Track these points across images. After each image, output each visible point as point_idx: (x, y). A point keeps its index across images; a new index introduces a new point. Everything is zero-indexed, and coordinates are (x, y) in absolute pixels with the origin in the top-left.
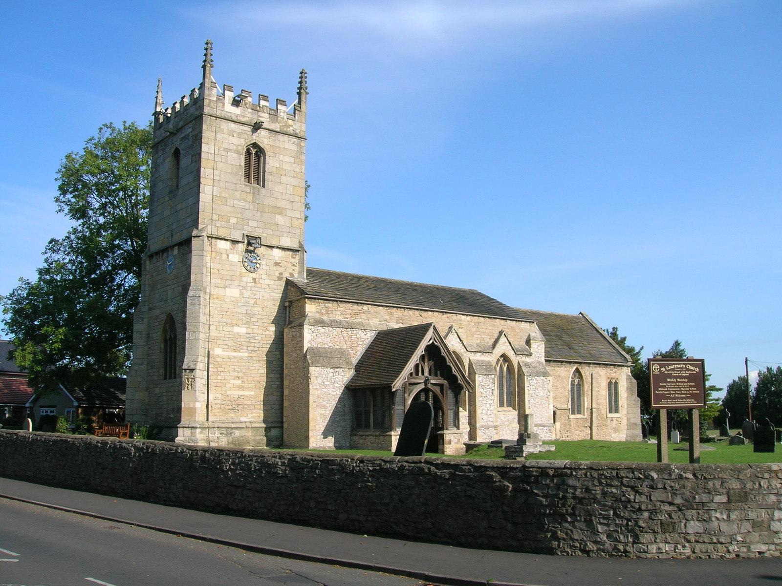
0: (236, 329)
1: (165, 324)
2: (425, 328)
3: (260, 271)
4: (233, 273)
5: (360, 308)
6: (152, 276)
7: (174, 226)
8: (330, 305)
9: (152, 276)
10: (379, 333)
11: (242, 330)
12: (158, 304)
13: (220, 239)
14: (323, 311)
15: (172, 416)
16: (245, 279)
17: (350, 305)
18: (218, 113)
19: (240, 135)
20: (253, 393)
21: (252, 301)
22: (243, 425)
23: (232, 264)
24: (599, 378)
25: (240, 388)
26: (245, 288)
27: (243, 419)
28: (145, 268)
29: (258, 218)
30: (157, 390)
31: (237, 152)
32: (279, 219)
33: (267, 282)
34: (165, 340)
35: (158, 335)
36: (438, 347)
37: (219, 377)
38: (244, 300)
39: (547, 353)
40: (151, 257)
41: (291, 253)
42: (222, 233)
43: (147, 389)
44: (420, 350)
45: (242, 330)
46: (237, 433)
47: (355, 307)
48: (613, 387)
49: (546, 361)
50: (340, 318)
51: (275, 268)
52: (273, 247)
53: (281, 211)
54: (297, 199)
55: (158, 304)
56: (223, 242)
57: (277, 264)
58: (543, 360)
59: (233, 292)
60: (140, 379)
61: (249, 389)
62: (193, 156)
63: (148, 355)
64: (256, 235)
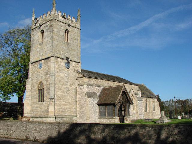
0: (63, 86)
1: (38, 85)
2: (121, 87)
3: (70, 69)
4: (62, 69)
5: (98, 80)
6: (32, 70)
7: (42, 54)
8: (91, 79)
9: (32, 70)
10: (103, 89)
11: (65, 86)
12: (35, 78)
13: (59, 58)
14: (89, 81)
15: (42, 114)
16: (66, 71)
17: (96, 79)
18: (57, 19)
19: (64, 26)
20: (68, 106)
21: (67, 78)
22: (66, 116)
23: (62, 66)
24: (151, 100)
25: (65, 105)
26: (65, 73)
27: (65, 114)
28: (30, 67)
29: (69, 52)
30: (35, 106)
31: (63, 31)
32: (74, 53)
33: (71, 72)
34: (39, 90)
35: (36, 89)
36: (125, 92)
37: (59, 101)
38: (65, 77)
39: (142, 94)
40: (32, 63)
41: (77, 63)
42: (59, 56)
43: (31, 105)
44: (121, 93)
45: (65, 86)
46: (64, 119)
47: (97, 80)
48: (154, 104)
49: (142, 97)
50: (93, 83)
51: (73, 68)
52: (73, 61)
53: (74, 50)
54: (79, 47)
55: (35, 78)
56: (59, 59)
57: (74, 66)
58: (140, 96)
59: (62, 75)
60: (28, 102)
61: (67, 105)
62: (49, 32)
63: (31, 95)
64: (68, 57)
